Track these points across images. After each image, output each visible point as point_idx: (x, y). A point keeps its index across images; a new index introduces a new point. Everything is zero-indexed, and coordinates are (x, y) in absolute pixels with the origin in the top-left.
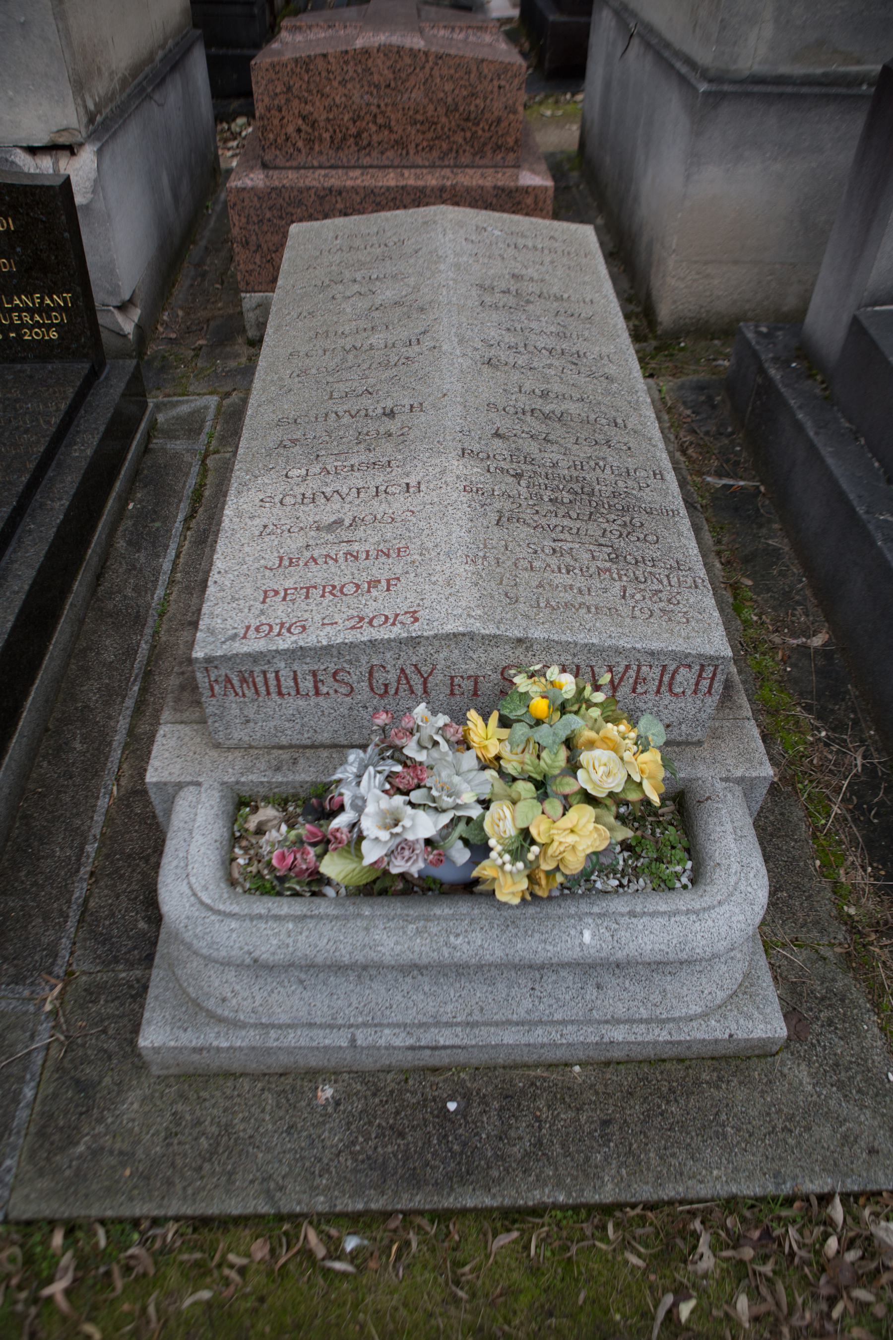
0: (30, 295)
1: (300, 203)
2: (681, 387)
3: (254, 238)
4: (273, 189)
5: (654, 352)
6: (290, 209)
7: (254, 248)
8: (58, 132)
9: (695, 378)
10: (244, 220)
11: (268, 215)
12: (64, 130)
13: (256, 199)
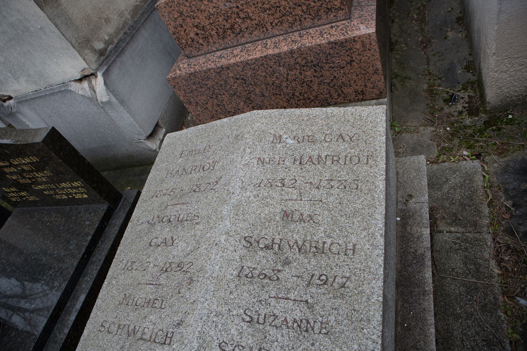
0: (65, 182)
1: (208, 78)
2: (505, 170)
3: (192, 99)
4: (190, 74)
5: (483, 126)
6: (204, 82)
7: (195, 104)
8: (82, 71)
9: (518, 155)
10: (183, 92)
11: (194, 87)
12: (84, 69)
13: (184, 81)
